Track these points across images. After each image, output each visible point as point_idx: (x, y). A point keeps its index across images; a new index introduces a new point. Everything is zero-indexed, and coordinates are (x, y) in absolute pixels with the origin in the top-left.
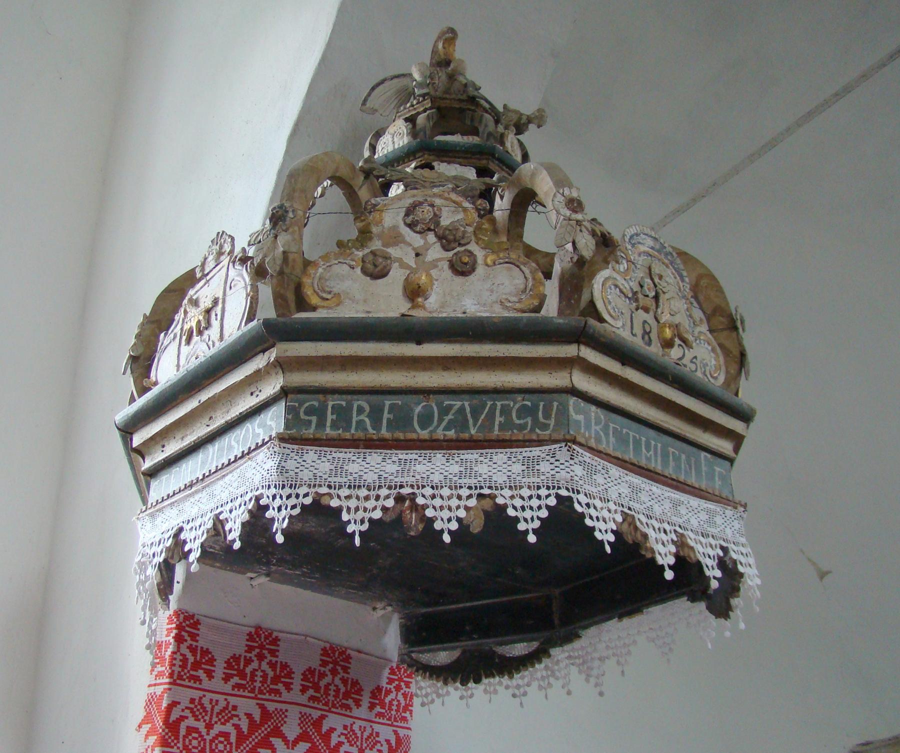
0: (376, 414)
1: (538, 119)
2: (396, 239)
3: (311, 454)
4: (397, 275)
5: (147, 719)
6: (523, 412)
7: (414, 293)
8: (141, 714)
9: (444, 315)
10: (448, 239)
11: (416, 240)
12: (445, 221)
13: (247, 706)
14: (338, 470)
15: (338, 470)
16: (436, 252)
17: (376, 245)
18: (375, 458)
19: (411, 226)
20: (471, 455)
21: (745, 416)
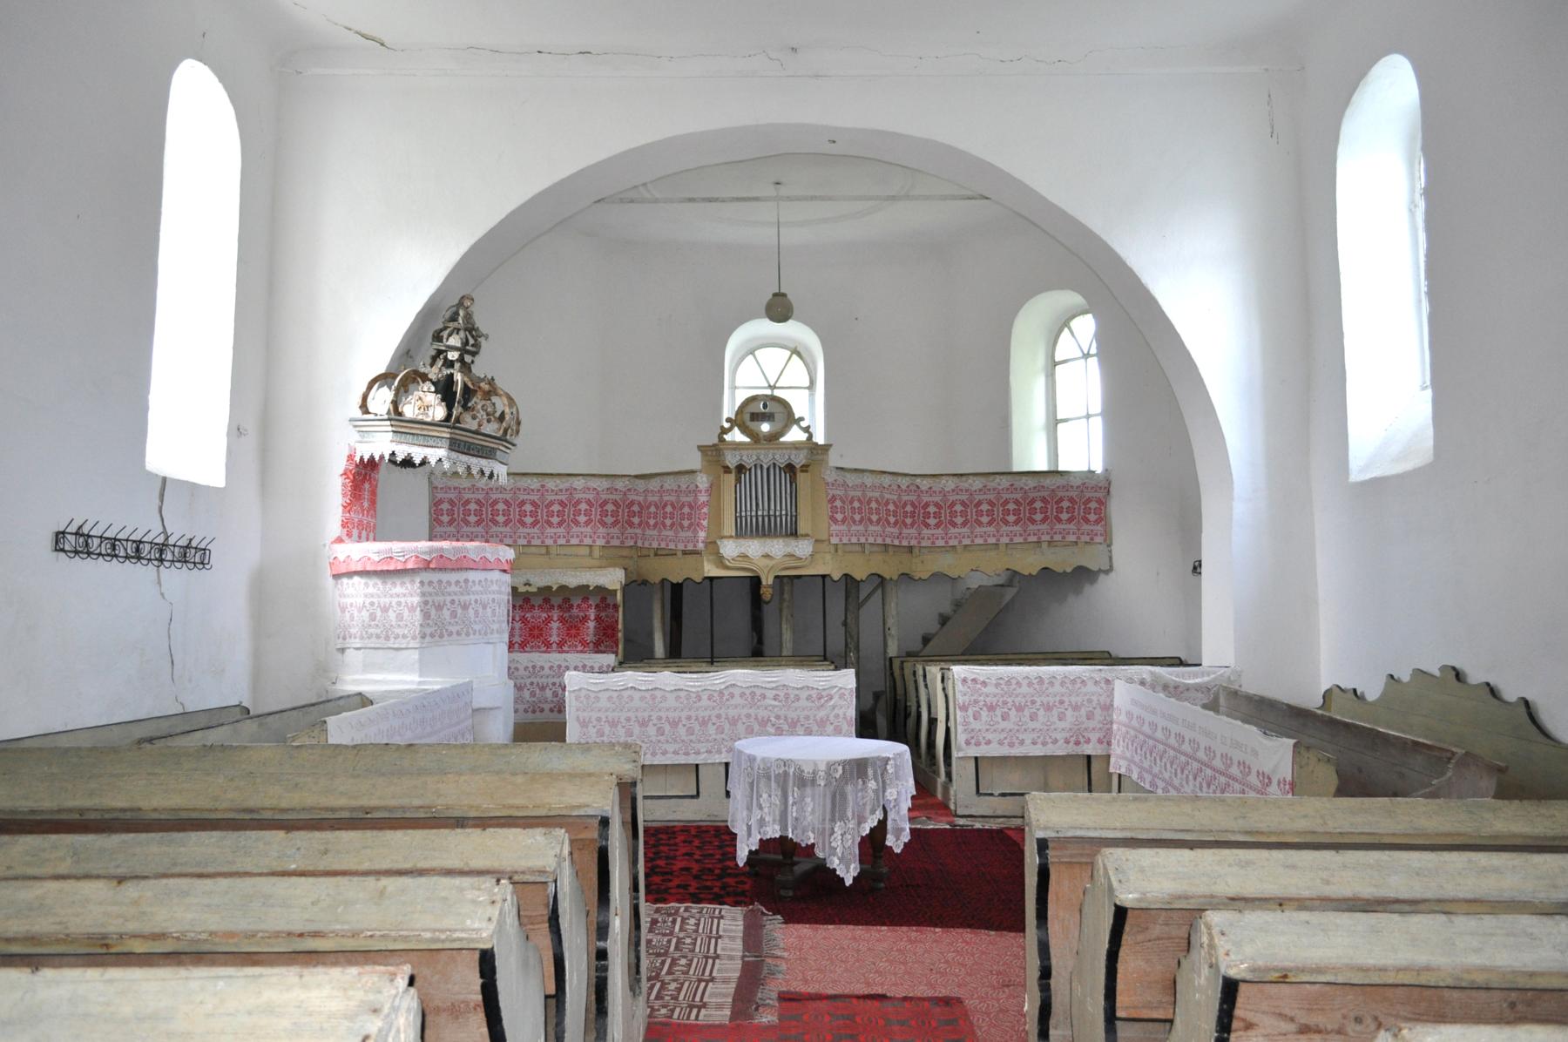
0: (465, 445)
1: (487, 337)
2: (478, 412)
3: (453, 453)
4: (478, 420)
5: (345, 474)
6: (490, 451)
7: (480, 425)
8: (341, 472)
9: (483, 431)
10: (488, 414)
11: (481, 411)
12: (489, 410)
13: (363, 472)
14: (458, 457)
15: (458, 457)
16: (485, 417)
17: (475, 412)
18: (464, 456)
19: (483, 410)
20: (479, 459)
21: (514, 445)
